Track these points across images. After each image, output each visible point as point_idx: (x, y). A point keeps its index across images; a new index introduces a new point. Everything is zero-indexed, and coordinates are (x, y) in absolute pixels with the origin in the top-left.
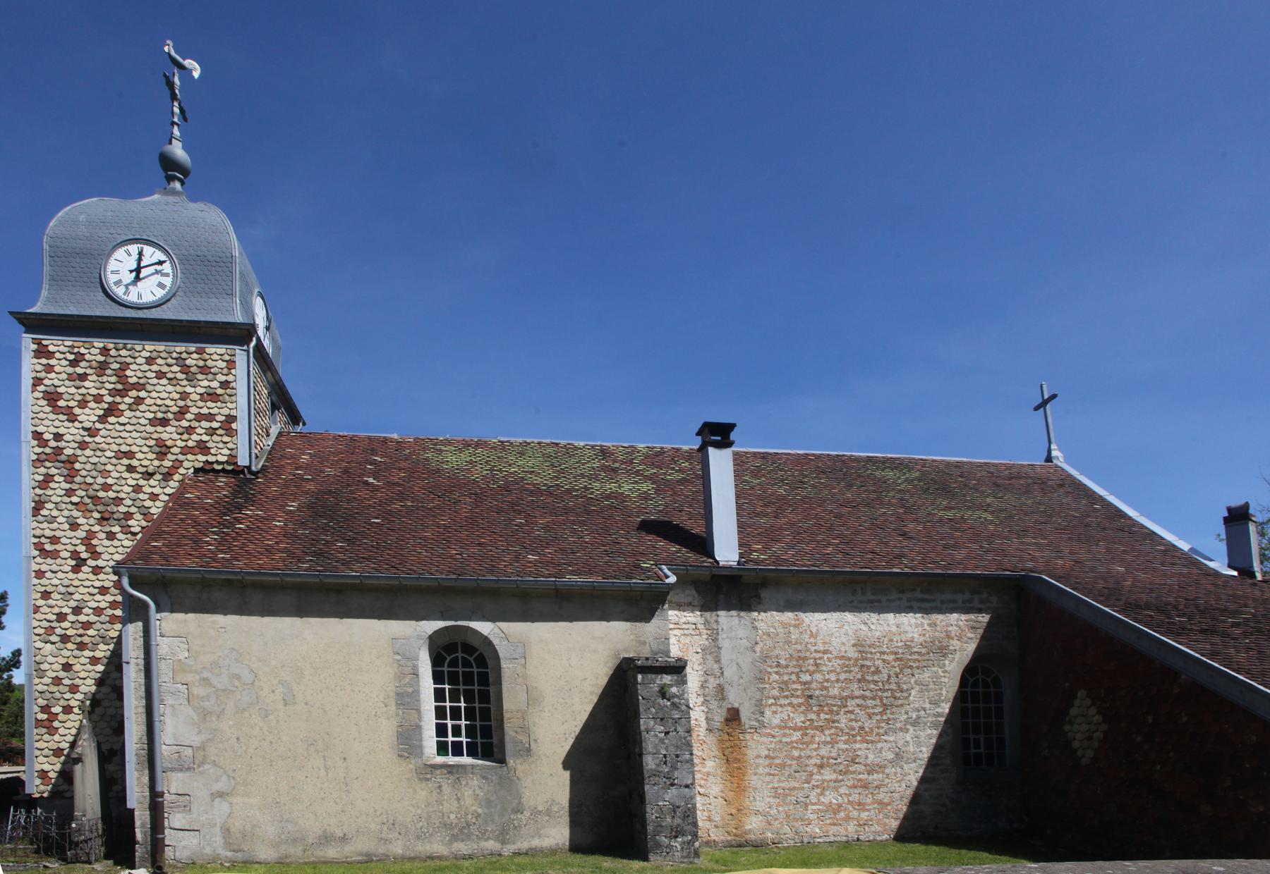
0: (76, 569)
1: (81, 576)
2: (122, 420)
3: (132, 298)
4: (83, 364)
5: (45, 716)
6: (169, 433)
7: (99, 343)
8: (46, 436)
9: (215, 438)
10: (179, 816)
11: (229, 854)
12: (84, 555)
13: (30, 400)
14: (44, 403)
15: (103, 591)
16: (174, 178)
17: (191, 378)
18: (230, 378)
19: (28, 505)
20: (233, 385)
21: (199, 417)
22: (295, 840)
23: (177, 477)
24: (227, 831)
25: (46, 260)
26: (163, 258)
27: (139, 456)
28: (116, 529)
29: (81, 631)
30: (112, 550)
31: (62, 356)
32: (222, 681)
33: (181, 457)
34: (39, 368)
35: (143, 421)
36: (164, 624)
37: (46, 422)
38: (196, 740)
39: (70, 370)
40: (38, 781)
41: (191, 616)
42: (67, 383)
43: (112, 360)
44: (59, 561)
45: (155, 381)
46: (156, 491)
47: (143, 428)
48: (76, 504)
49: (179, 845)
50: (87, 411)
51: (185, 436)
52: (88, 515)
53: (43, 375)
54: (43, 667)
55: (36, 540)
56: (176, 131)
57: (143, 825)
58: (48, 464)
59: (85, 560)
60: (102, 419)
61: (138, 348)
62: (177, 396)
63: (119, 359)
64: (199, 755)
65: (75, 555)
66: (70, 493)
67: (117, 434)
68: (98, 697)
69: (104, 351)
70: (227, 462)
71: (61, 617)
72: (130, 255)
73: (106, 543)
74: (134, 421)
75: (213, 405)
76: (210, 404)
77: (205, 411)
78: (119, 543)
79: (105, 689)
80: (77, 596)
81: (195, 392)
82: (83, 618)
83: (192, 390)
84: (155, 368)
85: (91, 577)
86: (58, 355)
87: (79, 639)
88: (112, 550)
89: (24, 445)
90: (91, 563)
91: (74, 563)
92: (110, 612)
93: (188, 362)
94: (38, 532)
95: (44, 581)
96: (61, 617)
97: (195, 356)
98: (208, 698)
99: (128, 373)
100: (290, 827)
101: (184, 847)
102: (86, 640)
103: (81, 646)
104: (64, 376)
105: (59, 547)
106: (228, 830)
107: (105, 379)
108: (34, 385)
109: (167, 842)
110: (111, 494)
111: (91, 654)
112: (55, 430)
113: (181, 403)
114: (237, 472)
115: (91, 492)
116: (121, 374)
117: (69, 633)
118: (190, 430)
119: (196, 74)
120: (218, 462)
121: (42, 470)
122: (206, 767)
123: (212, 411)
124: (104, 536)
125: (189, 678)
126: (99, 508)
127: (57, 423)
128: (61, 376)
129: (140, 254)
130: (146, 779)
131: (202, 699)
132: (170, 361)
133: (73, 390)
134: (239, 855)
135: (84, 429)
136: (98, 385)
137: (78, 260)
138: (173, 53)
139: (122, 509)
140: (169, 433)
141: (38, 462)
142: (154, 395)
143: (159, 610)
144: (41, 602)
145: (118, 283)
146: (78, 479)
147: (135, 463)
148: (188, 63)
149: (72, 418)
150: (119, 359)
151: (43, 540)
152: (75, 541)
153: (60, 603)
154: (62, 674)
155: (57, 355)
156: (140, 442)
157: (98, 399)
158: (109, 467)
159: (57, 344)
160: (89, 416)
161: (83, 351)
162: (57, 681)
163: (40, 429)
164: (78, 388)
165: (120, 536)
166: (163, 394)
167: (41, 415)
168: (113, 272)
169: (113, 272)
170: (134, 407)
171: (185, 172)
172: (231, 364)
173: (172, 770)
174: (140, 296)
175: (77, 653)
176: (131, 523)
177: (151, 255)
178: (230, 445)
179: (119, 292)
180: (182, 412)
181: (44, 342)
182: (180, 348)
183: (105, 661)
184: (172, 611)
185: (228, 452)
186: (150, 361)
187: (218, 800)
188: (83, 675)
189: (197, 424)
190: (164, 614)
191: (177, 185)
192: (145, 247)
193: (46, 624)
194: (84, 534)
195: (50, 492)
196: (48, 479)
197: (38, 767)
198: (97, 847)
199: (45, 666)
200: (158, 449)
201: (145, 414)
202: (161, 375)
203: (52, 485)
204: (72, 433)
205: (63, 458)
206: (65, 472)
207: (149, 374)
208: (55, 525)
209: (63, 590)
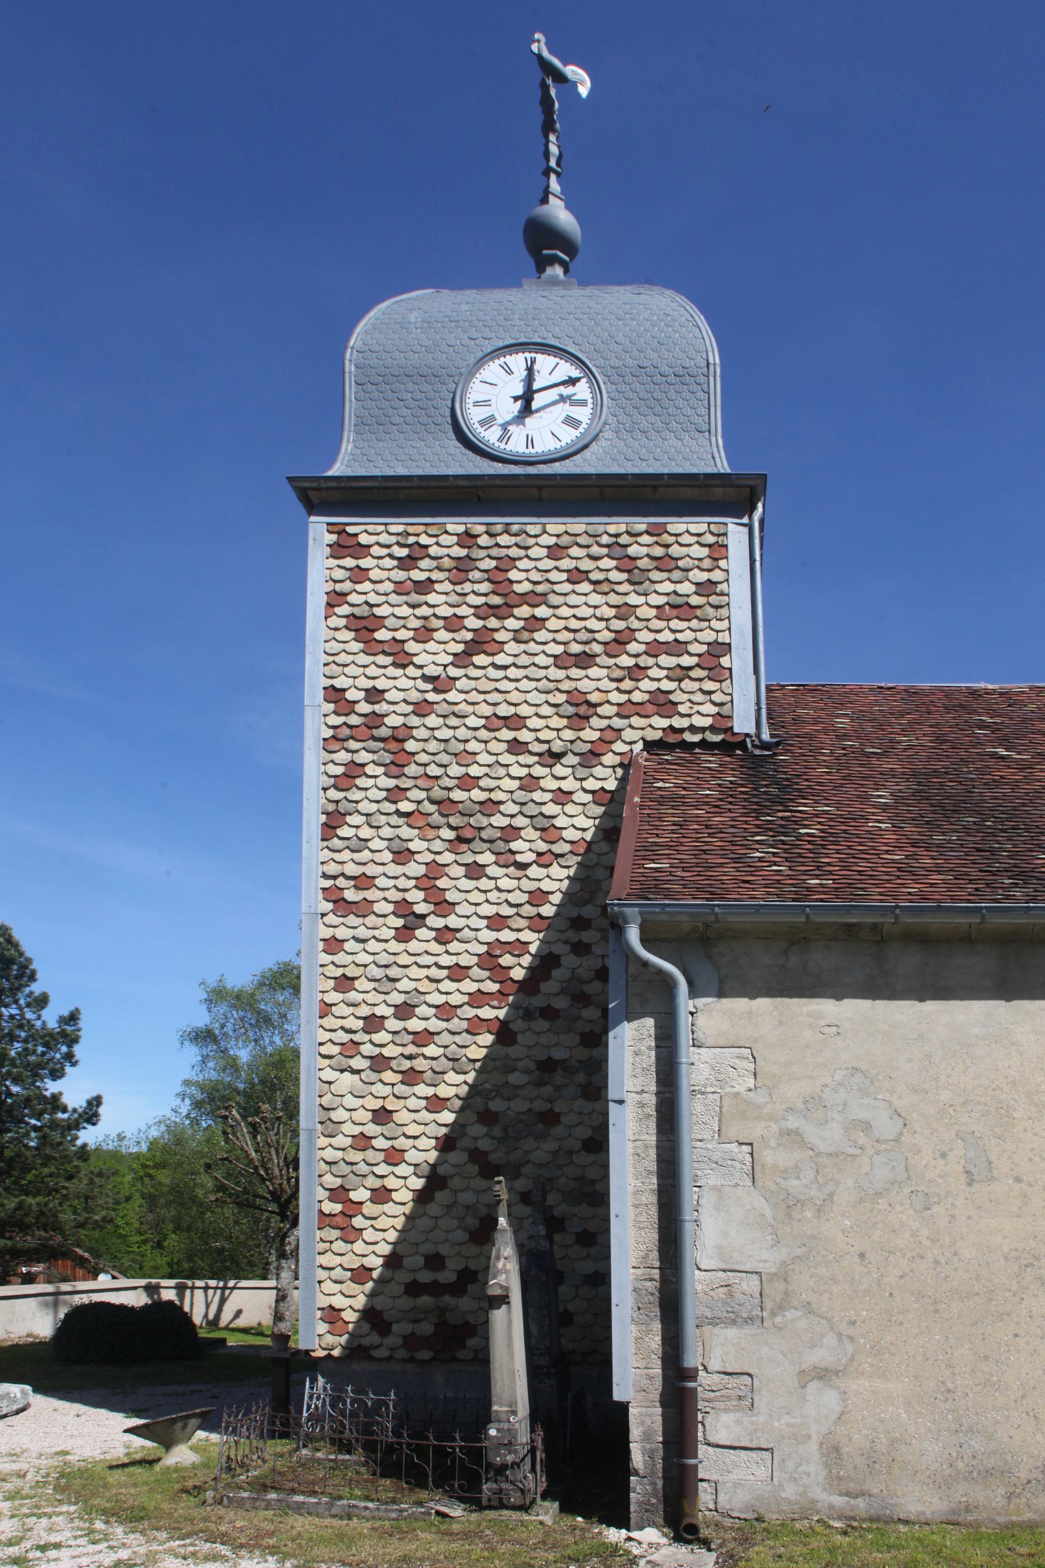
0: (404, 934)
1: (413, 946)
2: (501, 659)
3: (516, 445)
4: (425, 563)
5: (338, 1208)
6: (592, 682)
7: (456, 525)
8: (351, 695)
9: (687, 684)
10: (726, 1418)
11: (838, 1501)
12: (421, 908)
13: (321, 633)
14: (349, 635)
15: (457, 973)
16: (553, 260)
17: (637, 578)
18: (717, 575)
19: (313, 820)
20: (723, 587)
21: (655, 649)
22: (988, 1472)
23: (609, 759)
24: (832, 1453)
25: (350, 390)
26: (575, 373)
27: (534, 723)
28: (486, 858)
29: (411, 1049)
30: (476, 897)
31: (384, 552)
32: (829, 1136)
33: (617, 723)
34: (339, 574)
35: (542, 660)
36: (701, 1021)
37: (352, 670)
38: (767, 1259)
39: (400, 575)
40: (322, 1328)
41: (763, 1003)
42: (394, 598)
43: (482, 553)
44: (371, 920)
45: (567, 587)
46: (568, 785)
47: (541, 673)
48: (408, 815)
49: (728, 1481)
50: (431, 646)
51: (627, 684)
52: (431, 833)
53: (347, 586)
54: (335, 1116)
55: (328, 883)
56: (554, 185)
57: (647, 1437)
58: (353, 745)
59: (423, 917)
60: (462, 659)
61: (533, 530)
62: (611, 613)
63: (495, 552)
64: (775, 1291)
65: (403, 908)
66: (394, 795)
67: (492, 685)
68: (441, 1171)
69: (467, 539)
70: (712, 729)
71: (373, 1023)
72: (510, 372)
73: (466, 884)
74: (524, 660)
75: (684, 625)
76: (675, 624)
77: (666, 636)
78: (490, 884)
79: (457, 1157)
80: (405, 985)
81: (645, 605)
82: (415, 1025)
83: (641, 600)
84: (566, 564)
85: (434, 947)
86: (376, 551)
87: (406, 1064)
88: (476, 897)
89: (308, 713)
90: (437, 922)
91: (400, 922)
92: (469, 1012)
93: (632, 551)
94: (332, 869)
95: (341, 958)
96: (373, 1023)
97: (646, 539)
98: (796, 1171)
99: (513, 575)
100: (976, 1444)
101: (738, 1484)
102: (420, 1064)
103: (411, 1077)
104: (389, 587)
105: (371, 894)
106: (837, 1449)
107: (467, 587)
108: (330, 605)
109: (700, 1476)
110: (477, 795)
111: (430, 1091)
112: (369, 684)
113: (618, 625)
114: (732, 746)
115: (437, 793)
116: (499, 579)
117: (388, 1052)
118: (636, 672)
119: (584, 91)
120: (693, 729)
121: (343, 756)
122: (790, 1315)
123: (680, 637)
124: (460, 871)
125: (755, 1130)
126: (452, 820)
127: (372, 671)
128: (380, 588)
129: (530, 370)
130: (655, 1341)
131: (784, 1173)
132: (595, 550)
133: (405, 611)
134: (861, 1504)
135: (425, 678)
136: (454, 599)
137: (411, 386)
138: (546, 54)
139: (499, 821)
140: (592, 682)
141: (336, 740)
142: (564, 611)
143: (694, 992)
144: (333, 997)
145: (488, 422)
146: (412, 770)
147: (525, 736)
148: (572, 71)
149: (402, 660)
150: (495, 552)
151: (341, 882)
152: (402, 883)
153: (371, 998)
154: (371, 1129)
155: (376, 551)
156: (535, 697)
157: (453, 624)
158: (473, 746)
159: (369, 530)
160: (435, 655)
161: (424, 540)
162: (362, 1142)
163: (340, 683)
164: (414, 606)
165: (493, 871)
166: (584, 610)
167: (343, 658)
168: (477, 404)
169: (477, 404)
170: (525, 635)
171: (569, 246)
172: (718, 550)
173: (713, 1322)
174: (530, 442)
175: (401, 1089)
176: (515, 846)
177: (550, 369)
178: (717, 697)
179: (491, 436)
180: (620, 641)
181: (350, 529)
182: (617, 525)
183: (458, 1104)
184: (721, 994)
185: (714, 710)
186: (556, 552)
187: (813, 1386)
188: (413, 1130)
189: (651, 661)
190: (701, 1002)
191: (558, 271)
192: (539, 357)
193: (342, 1037)
194: (422, 870)
195: (355, 795)
196: (354, 771)
197: (323, 1301)
198: (534, 1481)
199: (339, 1115)
200: (571, 710)
201: (547, 645)
202: (576, 576)
203: (361, 782)
204: (401, 686)
205: (383, 732)
206: (388, 758)
207: (554, 576)
208: (365, 855)
209: (377, 972)
